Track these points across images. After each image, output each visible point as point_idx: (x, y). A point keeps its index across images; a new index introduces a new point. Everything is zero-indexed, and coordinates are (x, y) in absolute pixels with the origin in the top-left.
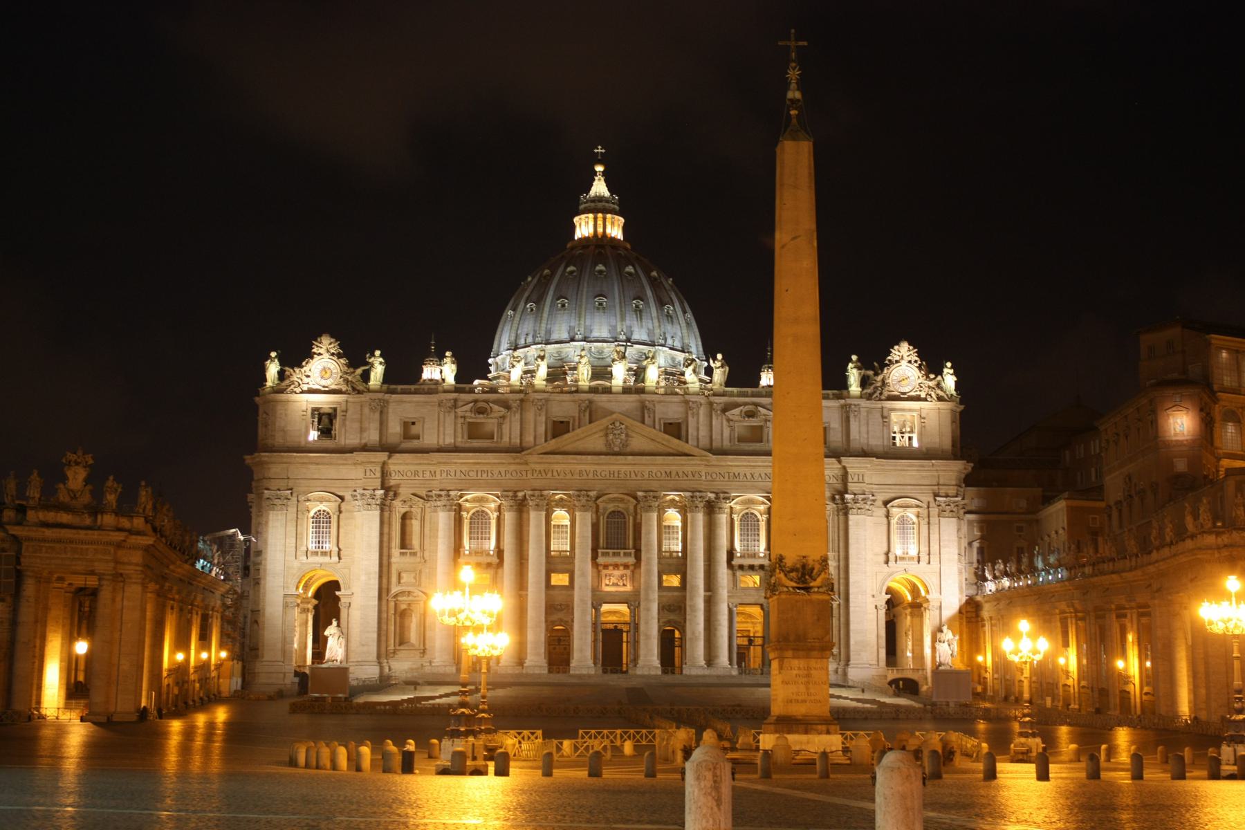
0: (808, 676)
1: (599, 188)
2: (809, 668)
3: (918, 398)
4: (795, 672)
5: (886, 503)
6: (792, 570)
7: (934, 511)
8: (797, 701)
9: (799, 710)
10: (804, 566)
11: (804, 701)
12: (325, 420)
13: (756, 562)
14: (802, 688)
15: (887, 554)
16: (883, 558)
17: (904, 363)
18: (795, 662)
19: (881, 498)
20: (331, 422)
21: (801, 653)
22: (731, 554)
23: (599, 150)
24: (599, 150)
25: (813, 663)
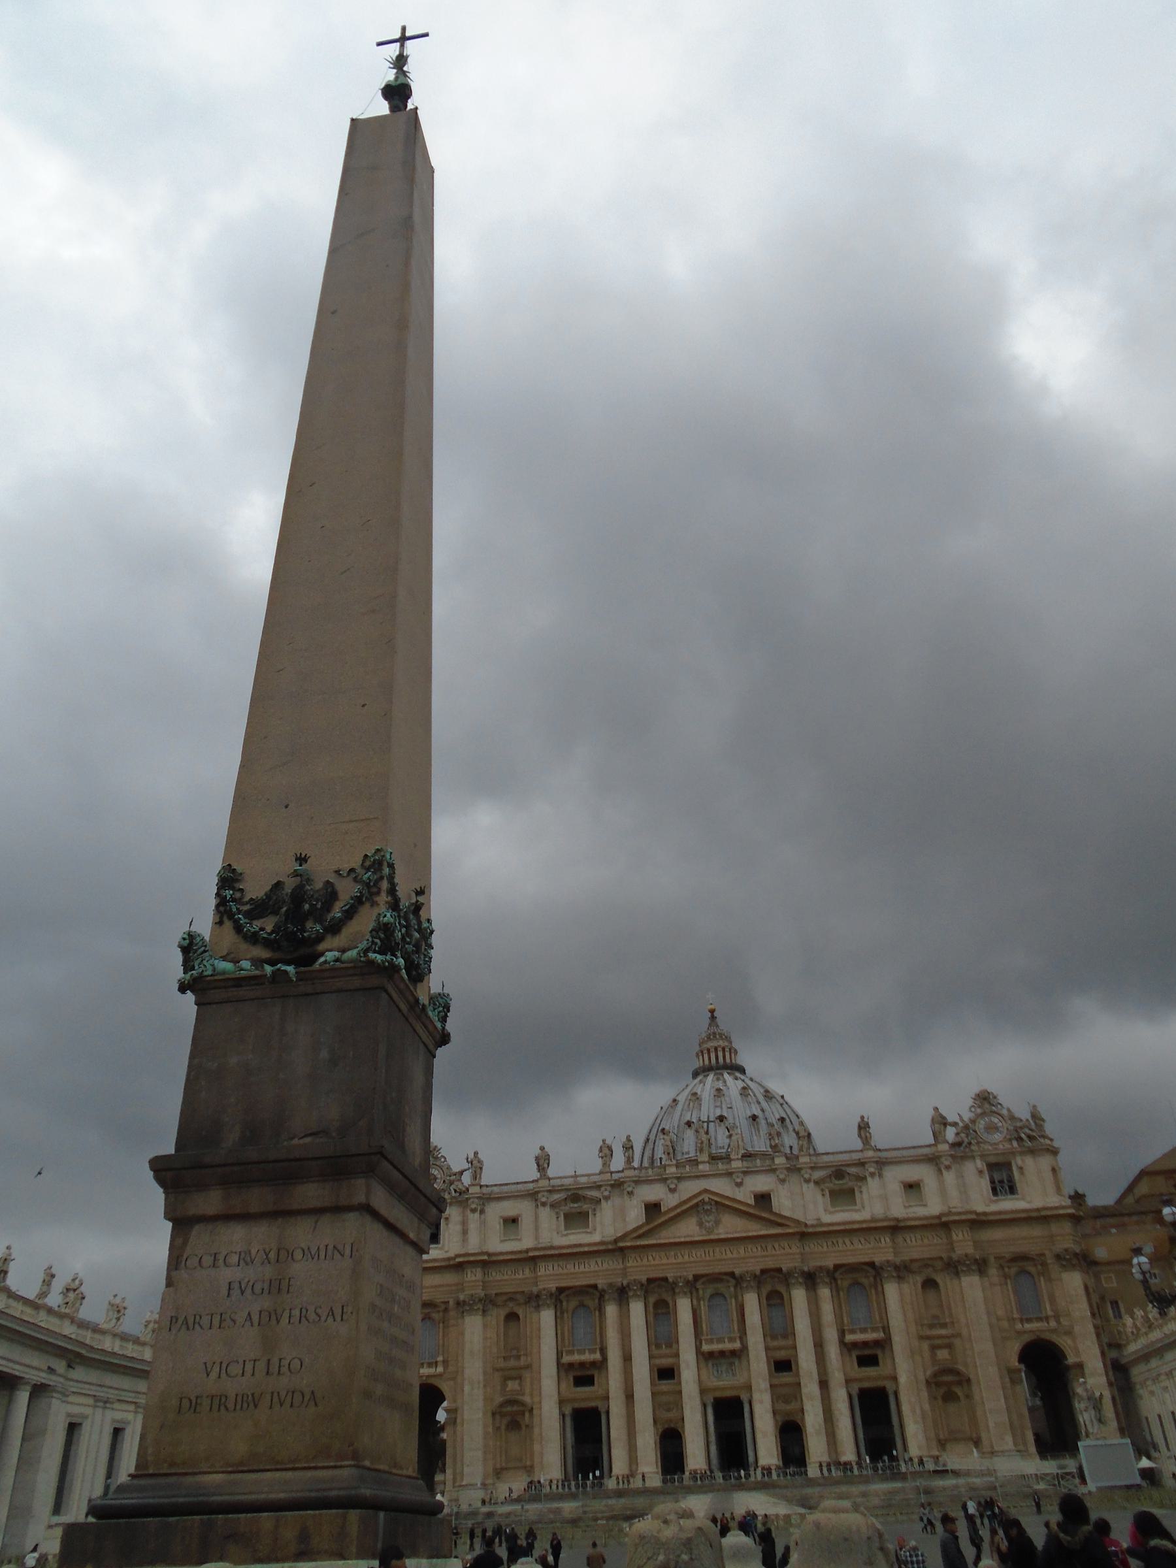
0: (278, 1286)
2: (284, 1255)
4: (227, 1274)
6: (260, 908)
8: (219, 1401)
10: (299, 895)
11: (250, 1401)
18: (235, 1236)
21: (256, 1198)
25: (301, 1233)
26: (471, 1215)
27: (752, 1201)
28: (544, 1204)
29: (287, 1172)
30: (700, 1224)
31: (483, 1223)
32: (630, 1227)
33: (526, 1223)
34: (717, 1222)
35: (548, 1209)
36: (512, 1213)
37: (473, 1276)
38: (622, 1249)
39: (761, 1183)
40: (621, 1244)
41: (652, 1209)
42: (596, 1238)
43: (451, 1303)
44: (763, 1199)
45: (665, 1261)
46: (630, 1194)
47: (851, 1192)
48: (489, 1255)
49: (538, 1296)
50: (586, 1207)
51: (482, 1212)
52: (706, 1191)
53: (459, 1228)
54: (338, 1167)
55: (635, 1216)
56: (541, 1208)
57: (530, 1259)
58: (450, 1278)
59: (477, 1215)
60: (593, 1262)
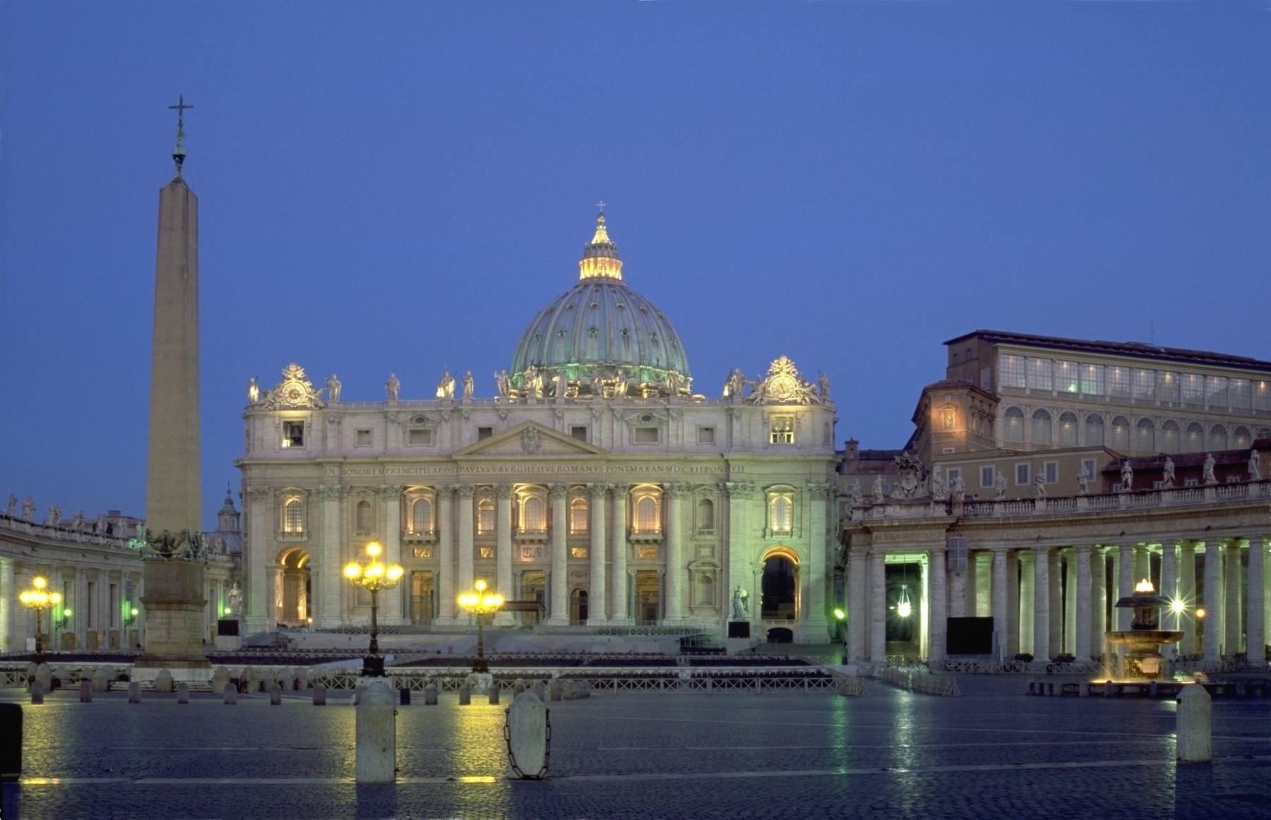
0: (169, 624)
1: (601, 236)
2: (170, 618)
3: (795, 403)
5: (764, 488)
7: (807, 496)
9: (160, 650)
12: (296, 430)
13: (650, 537)
14: (164, 633)
15: (764, 530)
16: (760, 533)
17: (783, 374)
18: (159, 613)
19: (759, 485)
20: (301, 432)
22: (629, 531)
23: (602, 204)
24: (602, 204)
25: (173, 614)
26: (329, 426)
27: (568, 432)
28: (393, 422)
29: (170, 603)
30: (523, 446)
31: (340, 432)
32: (466, 444)
33: (377, 434)
34: (538, 446)
35: (395, 425)
36: (364, 427)
37: (332, 473)
38: (455, 461)
39: (580, 418)
40: (454, 458)
41: (485, 432)
42: (436, 449)
43: (314, 491)
44: (579, 431)
45: (491, 472)
46: (467, 419)
47: (654, 430)
48: (345, 458)
49: (385, 491)
50: (428, 426)
51: (339, 423)
52: (531, 421)
53: (319, 435)
54: (180, 603)
55: (469, 434)
56: (390, 425)
57: (379, 462)
58: (312, 472)
59: (334, 426)
60: (432, 469)
